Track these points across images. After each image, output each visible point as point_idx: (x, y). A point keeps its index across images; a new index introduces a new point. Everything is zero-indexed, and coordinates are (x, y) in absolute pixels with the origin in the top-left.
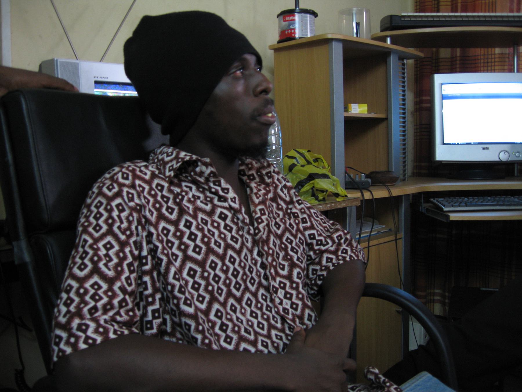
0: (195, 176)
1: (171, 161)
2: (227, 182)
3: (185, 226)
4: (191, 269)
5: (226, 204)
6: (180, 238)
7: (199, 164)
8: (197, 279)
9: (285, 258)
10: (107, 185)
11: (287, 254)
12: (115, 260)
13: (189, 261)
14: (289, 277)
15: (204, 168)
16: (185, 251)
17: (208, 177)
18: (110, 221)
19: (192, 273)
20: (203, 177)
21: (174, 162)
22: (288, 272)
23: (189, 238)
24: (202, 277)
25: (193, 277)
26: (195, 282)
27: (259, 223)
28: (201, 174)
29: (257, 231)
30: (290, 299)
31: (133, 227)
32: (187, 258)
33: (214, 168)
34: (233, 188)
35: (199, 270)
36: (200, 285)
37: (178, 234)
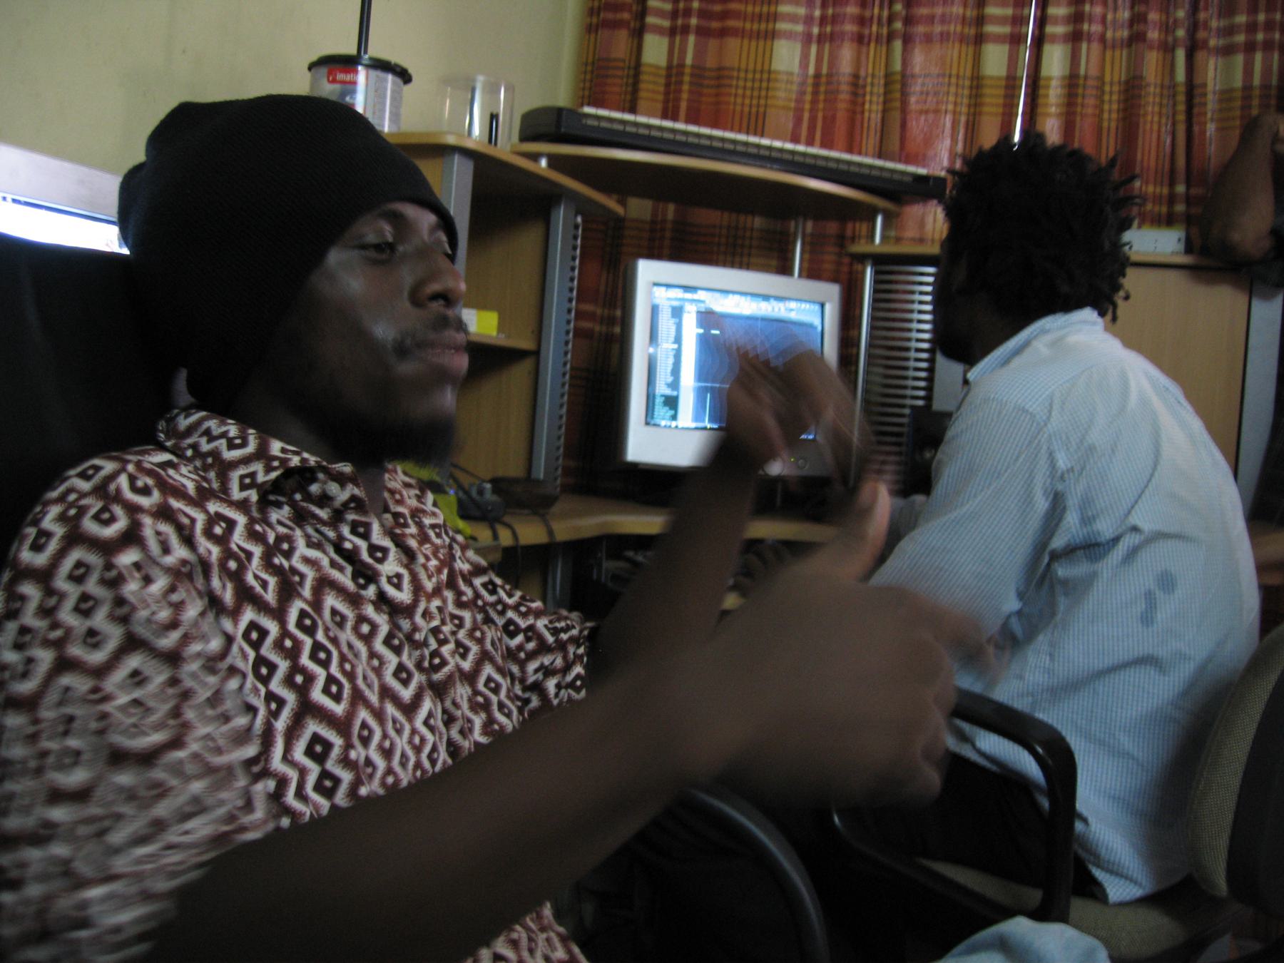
0: (305, 504)
1: (246, 461)
4: (316, 738)
7: (321, 476)
8: (330, 765)
10: (93, 511)
13: (314, 717)
15: (333, 488)
17: (342, 508)
19: (319, 749)
20: (329, 507)
21: (258, 467)
24: (346, 762)
25: (320, 759)
26: (325, 774)
28: (324, 500)
32: (307, 709)
33: (362, 489)
35: (337, 741)
36: (337, 781)
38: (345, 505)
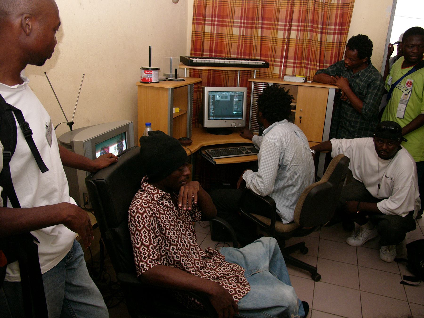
1: (156, 193)
12: (148, 237)
15: (167, 196)
18: (144, 223)
31: (151, 223)
38: (168, 199)
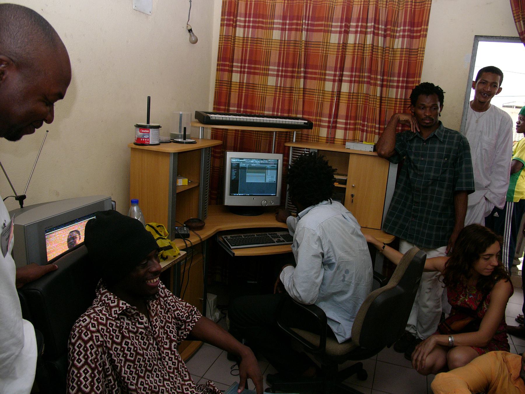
2: (143, 314)
3: (125, 344)
5: (143, 326)
6: (123, 351)
9: (167, 338)
11: (168, 335)
14: (170, 348)
15: (132, 311)
16: (125, 357)
22: (169, 346)
23: (127, 350)
27: (155, 328)
29: (155, 333)
30: (171, 360)
34: (145, 316)
37: (122, 349)
